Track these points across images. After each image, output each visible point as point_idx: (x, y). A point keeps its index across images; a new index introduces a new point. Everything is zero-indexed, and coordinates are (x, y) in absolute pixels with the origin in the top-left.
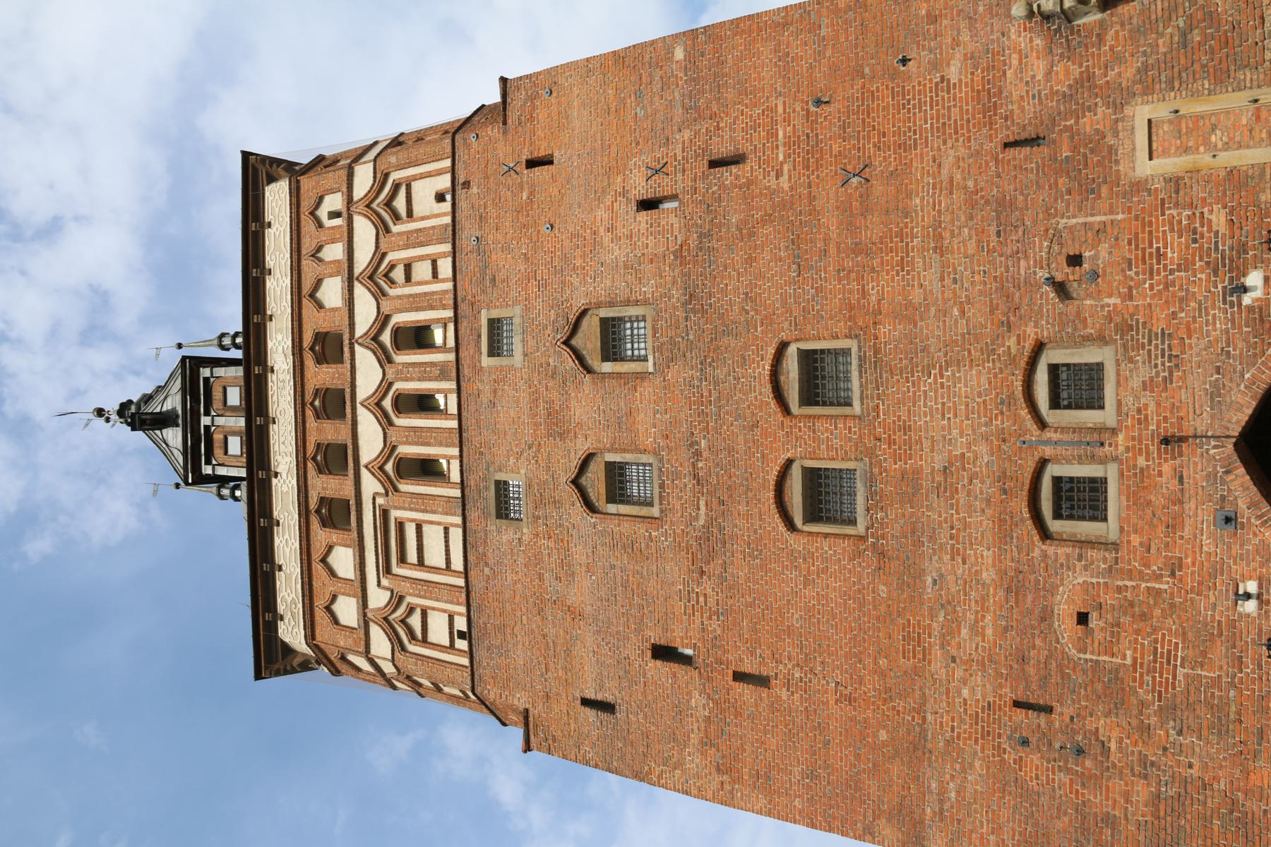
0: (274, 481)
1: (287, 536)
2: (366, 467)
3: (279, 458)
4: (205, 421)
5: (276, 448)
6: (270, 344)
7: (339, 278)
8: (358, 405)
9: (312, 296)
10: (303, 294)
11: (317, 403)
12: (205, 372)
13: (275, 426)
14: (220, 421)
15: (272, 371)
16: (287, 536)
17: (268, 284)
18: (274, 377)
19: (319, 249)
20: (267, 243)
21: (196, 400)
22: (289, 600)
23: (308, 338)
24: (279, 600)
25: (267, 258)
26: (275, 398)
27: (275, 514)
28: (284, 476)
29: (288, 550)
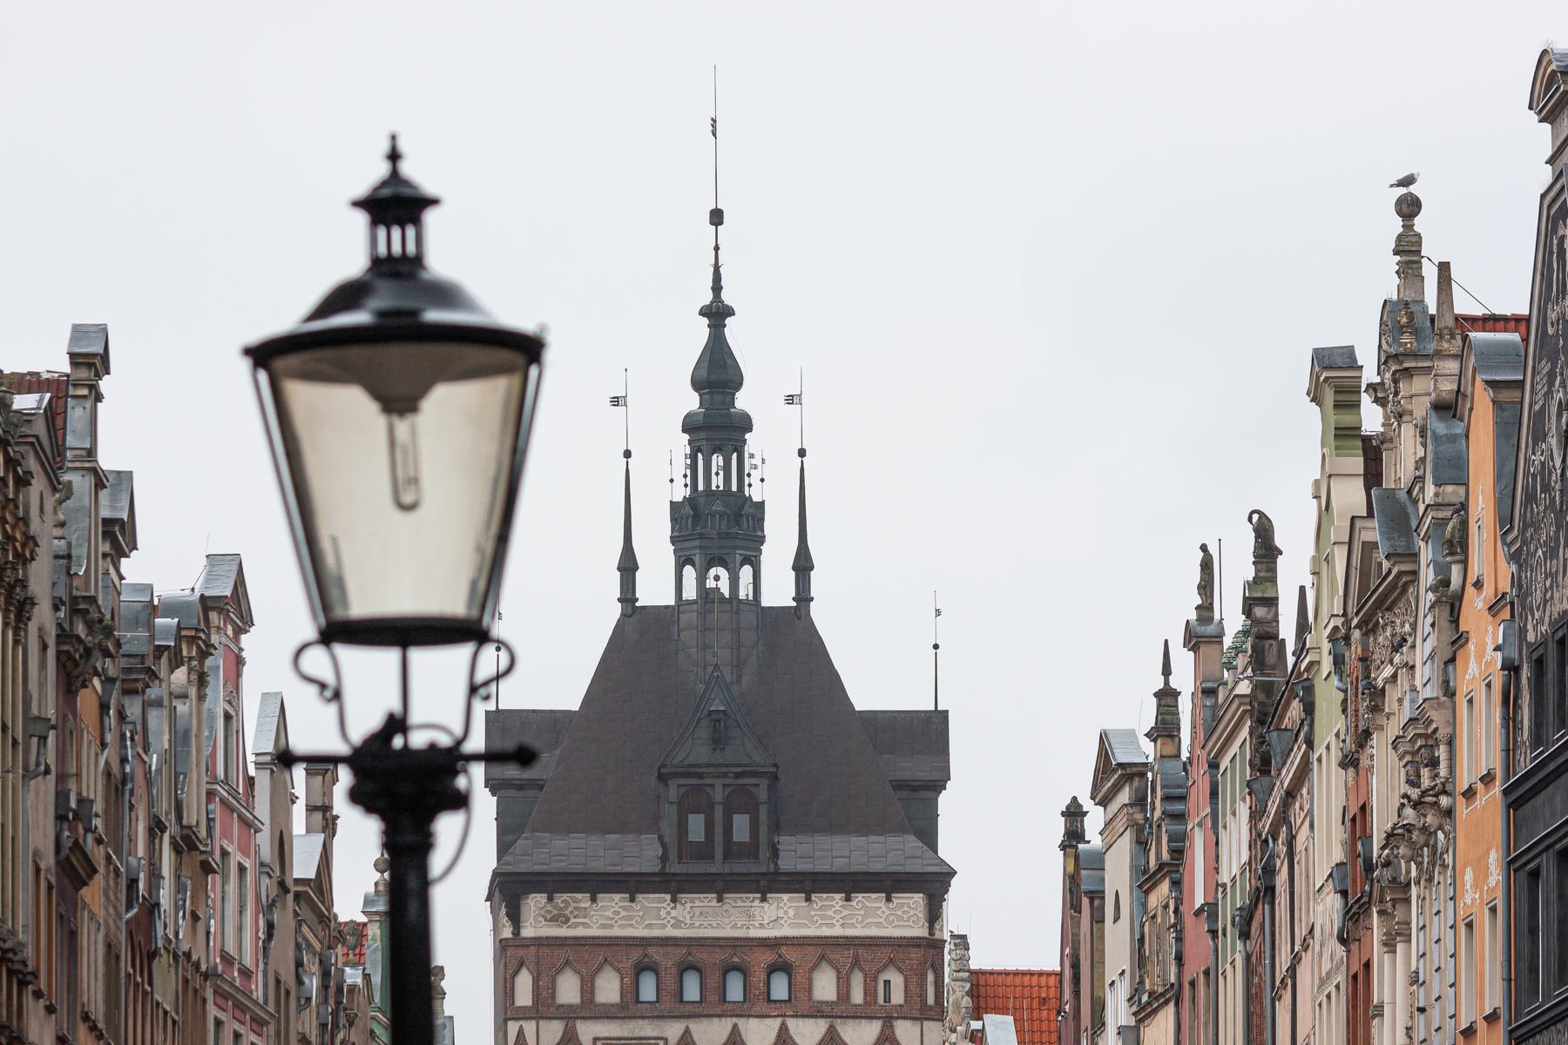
0: (668, 897)
1: (623, 913)
2: (687, 1031)
3: (688, 906)
4: (719, 783)
5: (698, 903)
6: (785, 897)
7: (834, 998)
8: (735, 1020)
9: (823, 957)
10: (826, 948)
11: (736, 959)
12: (762, 794)
13: (714, 903)
14: (719, 812)
15: (763, 900)
16: (623, 913)
17: (838, 896)
18: (757, 903)
19: (861, 970)
20: (874, 896)
21: (738, 775)
22: (567, 912)
23: (790, 955)
24: (565, 896)
25: (860, 896)
26: (740, 903)
27: (640, 897)
28: (674, 913)
29: (609, 913)
